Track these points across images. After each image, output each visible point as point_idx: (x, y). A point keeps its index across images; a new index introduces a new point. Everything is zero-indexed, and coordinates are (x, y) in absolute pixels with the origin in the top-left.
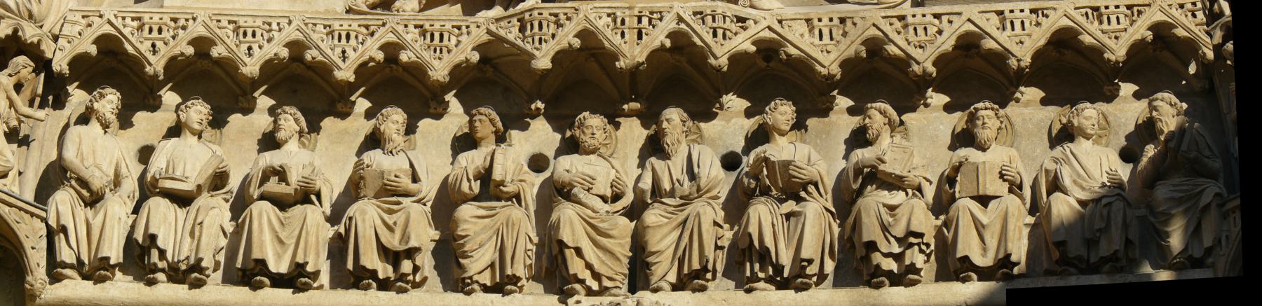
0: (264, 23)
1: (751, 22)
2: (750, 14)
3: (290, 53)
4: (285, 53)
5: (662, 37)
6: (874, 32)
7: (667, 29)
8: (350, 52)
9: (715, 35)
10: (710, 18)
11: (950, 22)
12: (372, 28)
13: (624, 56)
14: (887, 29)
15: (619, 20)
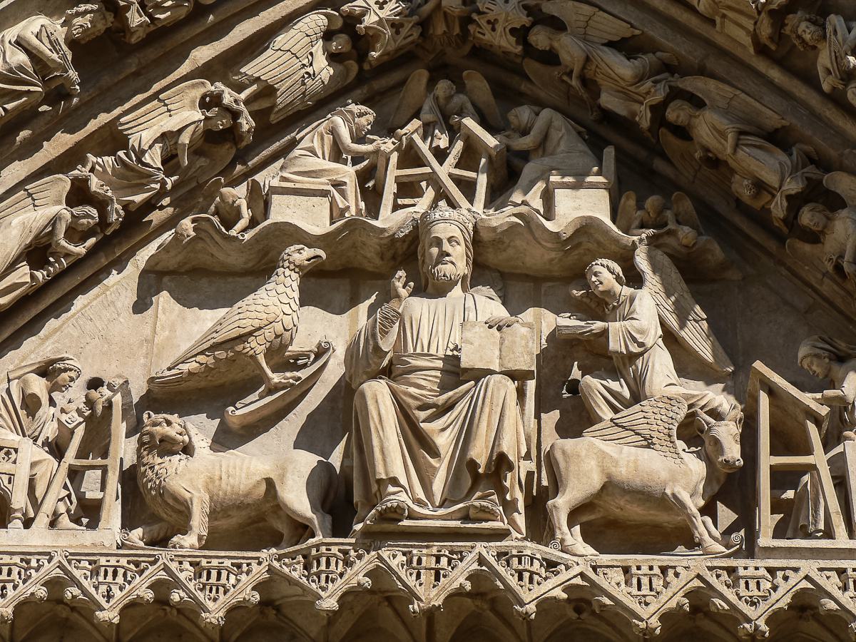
0: (22, 560)
1: (563, 567)
2: (562, 558)
3: (49, 592)
4: (42, 592)
5: (462, 580)
6: (697, 583)
7: (468, 570)
8: (115, 590)
9: (521, 578)
10: (515, 560)
11: (786, 578)
12: (143, 565)
13: (419, 599)
14: (712, 579)
15: (415, 559)
